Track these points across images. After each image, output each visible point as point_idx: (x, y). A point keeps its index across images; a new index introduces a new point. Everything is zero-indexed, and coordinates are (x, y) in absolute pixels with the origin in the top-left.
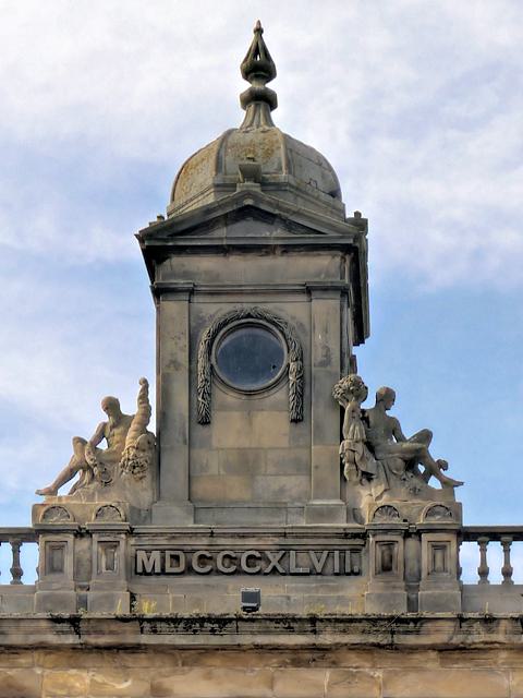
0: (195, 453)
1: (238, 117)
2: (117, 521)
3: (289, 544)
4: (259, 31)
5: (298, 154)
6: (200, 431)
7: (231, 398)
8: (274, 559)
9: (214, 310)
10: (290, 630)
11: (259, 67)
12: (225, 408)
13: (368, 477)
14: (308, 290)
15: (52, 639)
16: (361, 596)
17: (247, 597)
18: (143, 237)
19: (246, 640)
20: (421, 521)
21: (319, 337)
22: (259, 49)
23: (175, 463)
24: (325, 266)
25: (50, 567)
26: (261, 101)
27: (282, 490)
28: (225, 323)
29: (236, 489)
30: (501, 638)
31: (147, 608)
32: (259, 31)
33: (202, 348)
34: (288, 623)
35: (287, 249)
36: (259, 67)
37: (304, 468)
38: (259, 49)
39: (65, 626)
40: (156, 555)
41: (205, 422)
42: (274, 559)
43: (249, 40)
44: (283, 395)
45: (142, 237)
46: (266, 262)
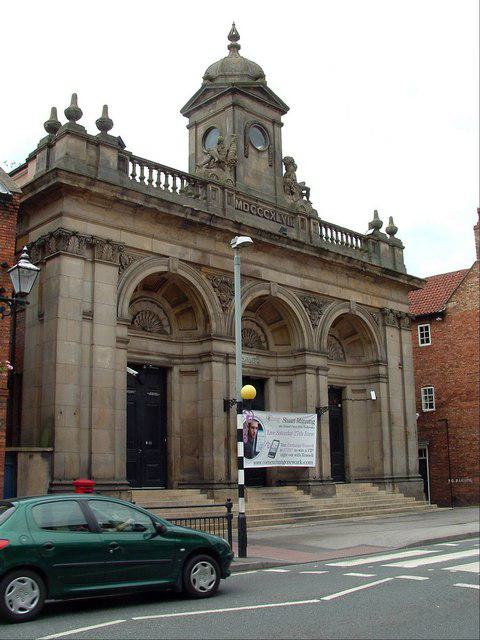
9: (252, 118)
11: (234, 37)
13: (292, 193)
22: (234, 29)
26: (234, 48)
36: (234, 37)
38: (234, 29)
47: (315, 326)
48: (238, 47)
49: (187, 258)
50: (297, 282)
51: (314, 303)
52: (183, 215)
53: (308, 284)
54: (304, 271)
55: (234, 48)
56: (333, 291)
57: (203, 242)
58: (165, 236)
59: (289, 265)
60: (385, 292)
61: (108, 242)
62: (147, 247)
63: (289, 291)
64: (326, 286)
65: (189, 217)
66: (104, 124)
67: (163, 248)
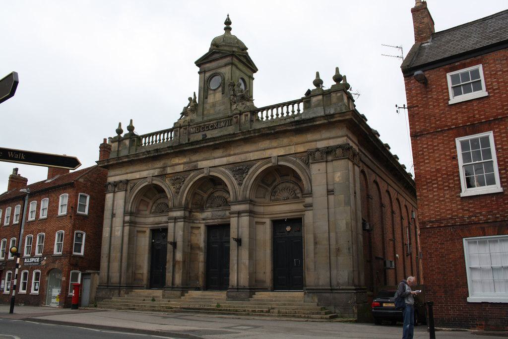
0: (204, 105)
1: (223, 32)
2: (187, 124)
3: (218, 121)
4: (228, 15)
5: (235, 38)
6: (205, 100)
7: (212, 92)
8: (215, 125)
9: (208, 75)
10: (210, 142)
11: (228, 23)
12: (211, 94)
14: (226, 65)
15: (169, 151)
16: (230, 130)
17: (203, 135)
18: (196, 63)
19: (202, 145)
20: (243, 110)
21: (227, 75)
23: (200, 110)
24: (228, 60)
25: (175, 135)
26: (228, 29)
27: (220, 110)
28: (210, 77)
29: (212, 112)
30: (252, 135)
31: (192, 140)
32: (228, 15)
33: (206, 82)
34: (214, 139)
35: (222, 58)
36: (228, 23)
37: (223, 103)
38: (228, 19)
39: (171, 148)
40: (194, 129)
41: (207, 98)
42: (215, 125)
43: (226, 17)
44: (220, 89)
45: (196, 63)
46: (218, 62)
47: (240, 184)
48: (230, 29)
49: (156, 174)
50: (224, 160)
51: (240, 170)
52: (144, 156)
53: (232, 159)
54: (228, 152)
55: (228, 29)
56: (252, 156)
57: (160, 164)
58: (145, 168)
59: (219, 153)
60: (310, 137)
61: (121, 181)
62: (138, 177)
63: (222, 169)
64: (247, 155)
65: (148, 156)
66: (131, 128)
67: (145, 174)
